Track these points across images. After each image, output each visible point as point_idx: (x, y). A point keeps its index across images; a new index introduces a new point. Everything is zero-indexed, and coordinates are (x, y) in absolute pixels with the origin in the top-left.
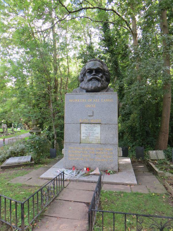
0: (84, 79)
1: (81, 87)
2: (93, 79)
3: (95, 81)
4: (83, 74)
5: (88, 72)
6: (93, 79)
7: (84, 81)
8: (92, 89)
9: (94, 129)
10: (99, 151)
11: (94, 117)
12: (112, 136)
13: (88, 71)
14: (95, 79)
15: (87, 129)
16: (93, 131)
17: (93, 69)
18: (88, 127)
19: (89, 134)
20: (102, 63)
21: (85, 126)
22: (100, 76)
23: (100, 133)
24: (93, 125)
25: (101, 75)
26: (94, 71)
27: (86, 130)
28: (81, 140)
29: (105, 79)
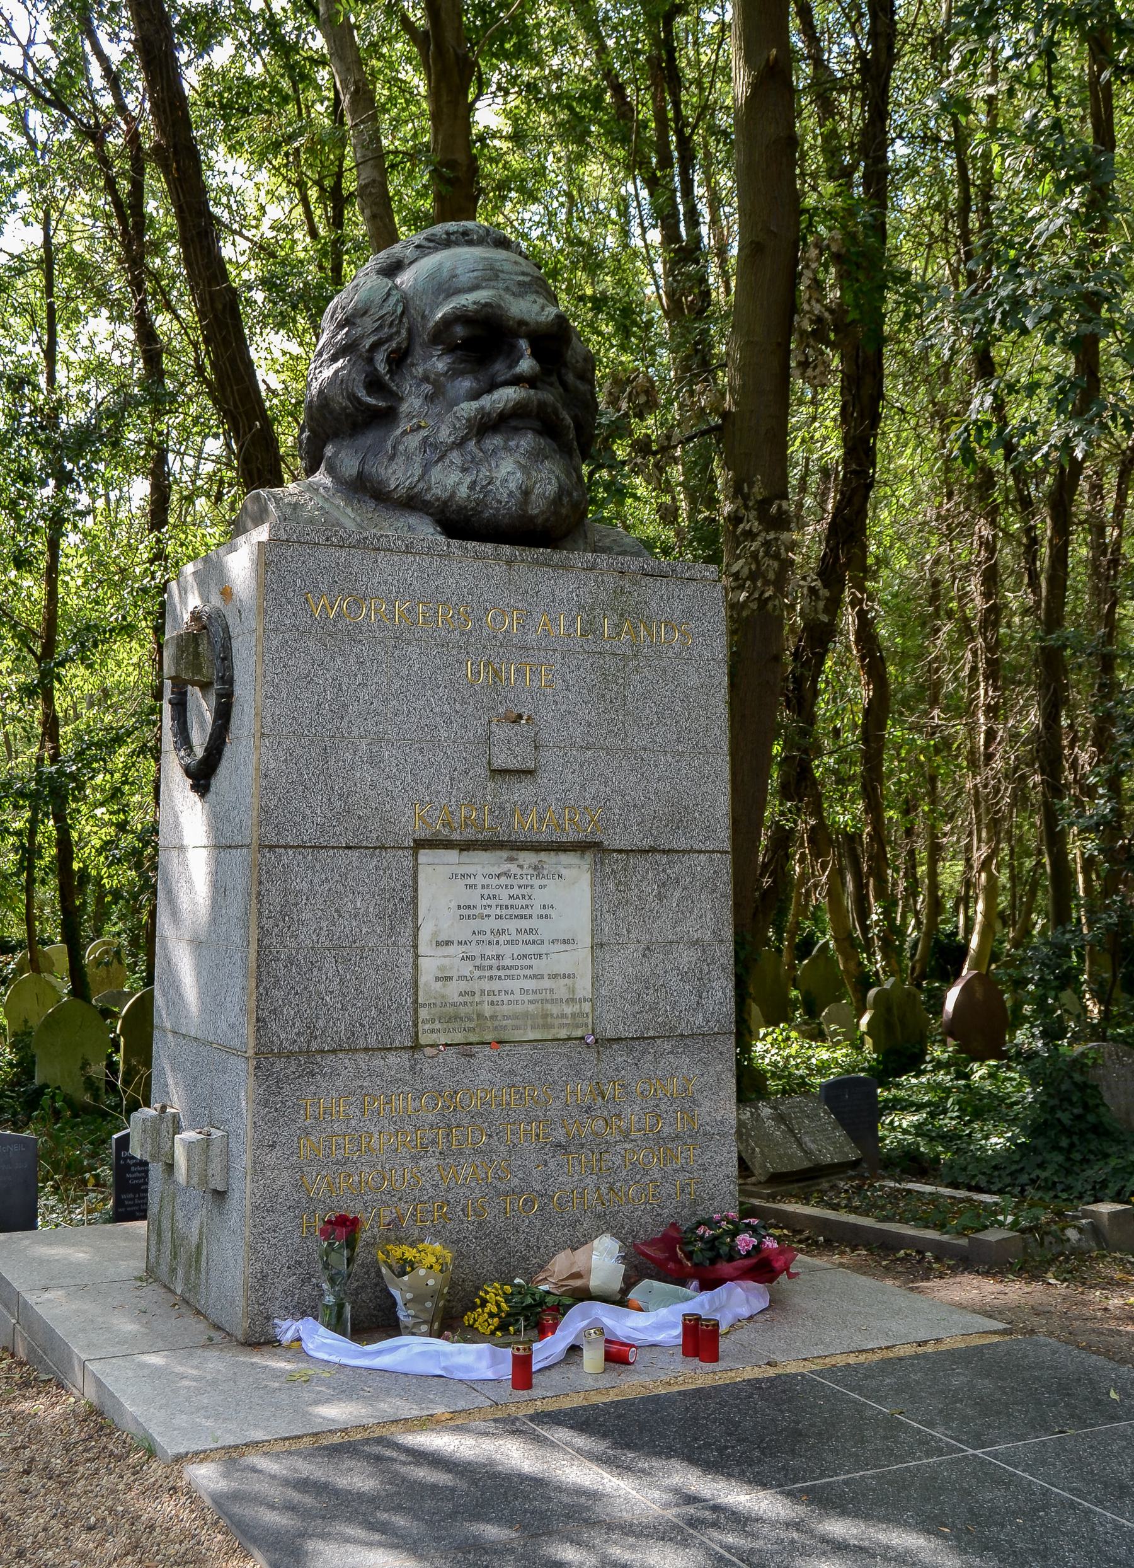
0: (404, 408)
4: (380, 357)
7: (404, 425)
8: (533, 511)
9: (540, 897)
10: (588, 1110)
11: (543, 779)
12: (687, 957)
13: (459, 331)
15: (474, 898)
16: (524, 924)
17: (522, 323)
18: (480, 881)
19: (491, 951)
21: (454, 876)
23: (585, 940)
24: (528, 858)
27: (466, 912)
28: (423, 1013)
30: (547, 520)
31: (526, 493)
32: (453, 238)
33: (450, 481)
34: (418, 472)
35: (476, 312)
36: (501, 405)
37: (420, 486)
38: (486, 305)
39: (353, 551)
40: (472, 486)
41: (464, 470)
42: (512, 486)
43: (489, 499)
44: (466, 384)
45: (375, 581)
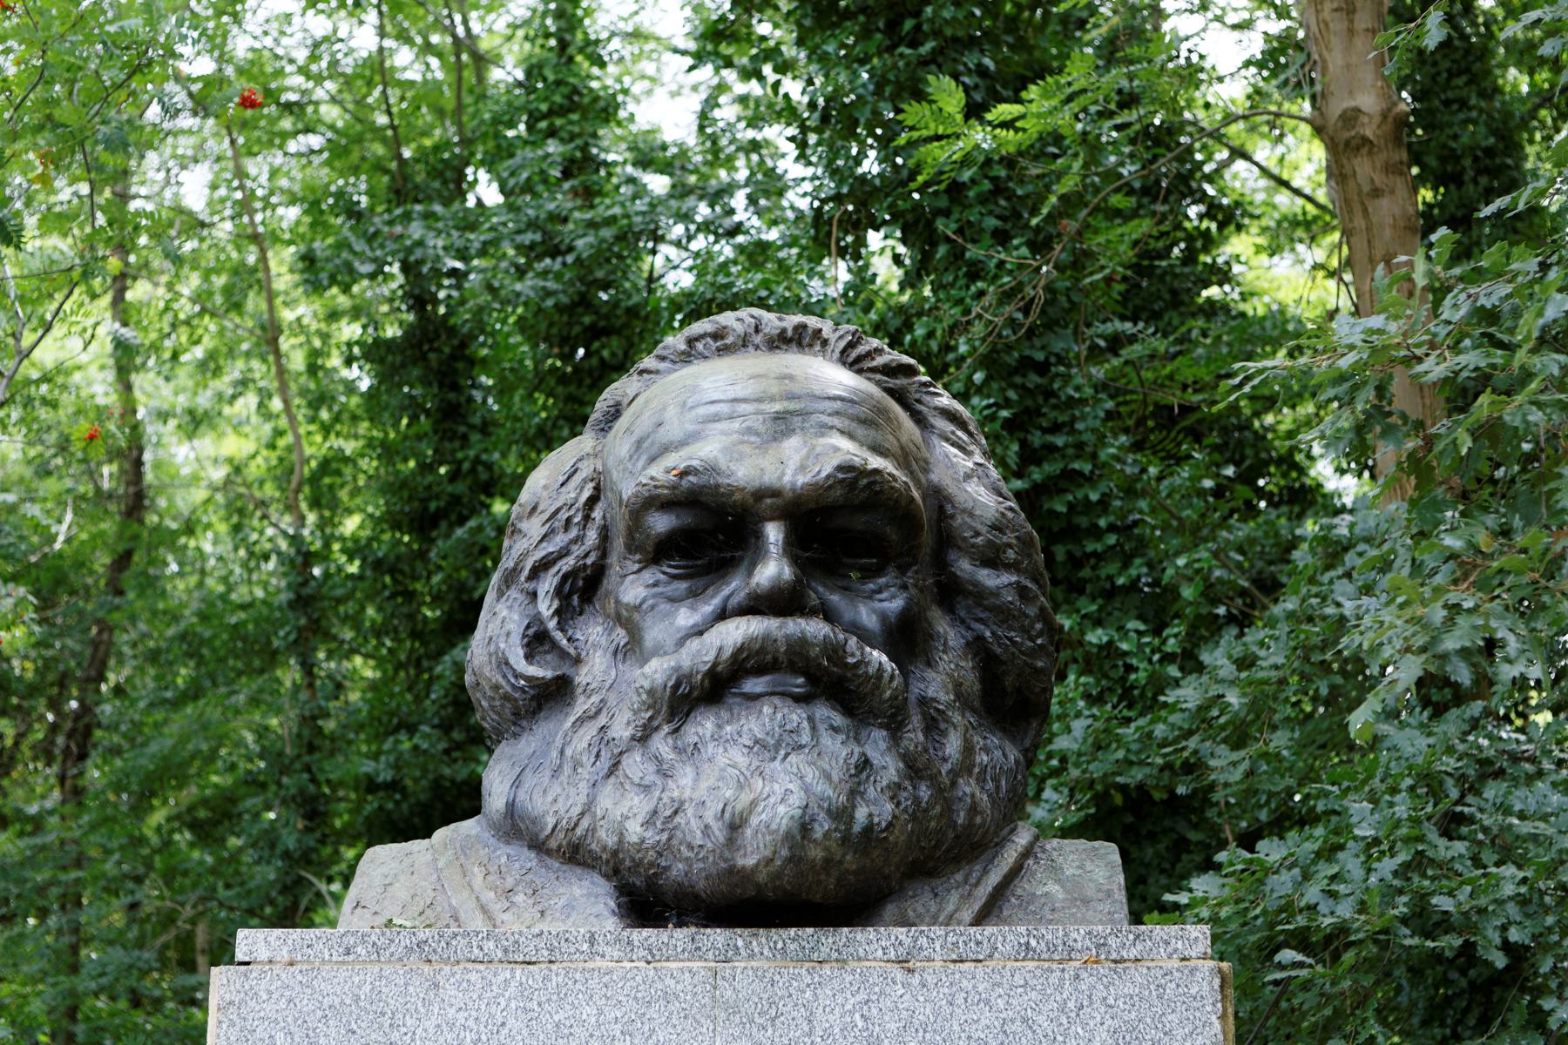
0: (582, 677)
1: (517, 828)
2: (753, 685)
3: (797, 716)
4: (548, 584)
5: (660, 552)
6: (760, 671)
7: (581, 705)
13: (661, 523)
14: (798, 683)
17: (760, 494)
20: (899, 396)
22: (867, 615)
25: (880, 604)
26: (774, 533)
29: (971, 680)
30: (778, 875)
31: (735, 826)
32: (700, 346)
33: (625, 815)
34: (582, 799)
35: (674, 487)
36: (710, 657)
37: (585, 823)
38: (684, 474)
39: (387, 971)
40: (648, 823)
41: (646, 789)
42: (709, 816)
43: (675, 842)
44: (685, 617)
45: (430, 1025)
